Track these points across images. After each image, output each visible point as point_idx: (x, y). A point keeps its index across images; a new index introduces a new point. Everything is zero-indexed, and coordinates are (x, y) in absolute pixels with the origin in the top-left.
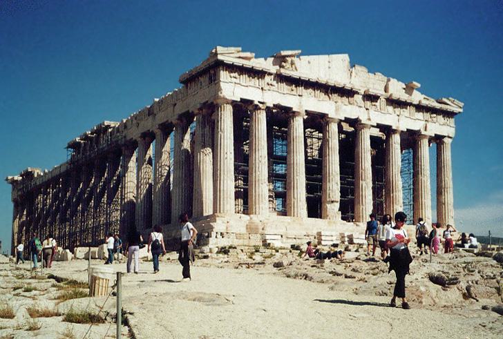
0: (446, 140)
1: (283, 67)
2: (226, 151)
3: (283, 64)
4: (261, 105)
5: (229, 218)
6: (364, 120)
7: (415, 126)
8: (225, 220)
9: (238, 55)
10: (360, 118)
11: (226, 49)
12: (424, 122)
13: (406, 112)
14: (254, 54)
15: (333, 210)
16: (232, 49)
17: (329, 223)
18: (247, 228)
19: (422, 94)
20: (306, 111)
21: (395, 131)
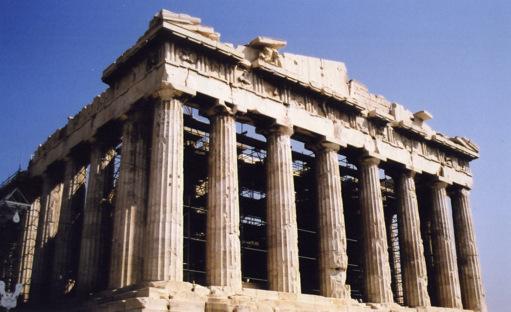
0: (464, 191)
1: (263, 59)
2: (169, 173)
4: (229, 109)
5: (174, 290)
6: (371, 149)
7: (433, 169)
8: (166, 292)
9: (195, 28)
10: (367, 148)
11: (177, 15)
12: (440, 165)
13: (419, 149)
14: (219, 35)
16: (185, 17)
20: (295, 127)
21: (408, 173)
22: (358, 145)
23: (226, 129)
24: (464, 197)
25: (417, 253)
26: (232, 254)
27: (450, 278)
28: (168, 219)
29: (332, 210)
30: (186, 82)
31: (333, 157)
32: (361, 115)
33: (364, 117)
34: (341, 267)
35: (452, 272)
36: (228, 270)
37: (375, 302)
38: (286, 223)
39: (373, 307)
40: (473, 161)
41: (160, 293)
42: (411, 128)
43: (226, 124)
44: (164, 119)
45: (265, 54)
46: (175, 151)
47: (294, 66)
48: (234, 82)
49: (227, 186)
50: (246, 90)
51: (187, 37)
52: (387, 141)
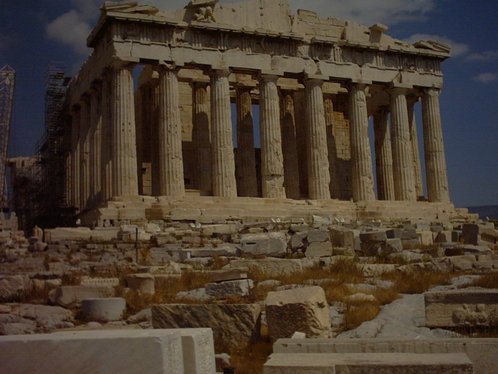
0: (431, 92)
1: (195, 19)
2: (122, 122)
3: (197, 15)
4: (168, 66)
9: (134, 9)
10: (307, 72)
12: (397, 72)
15: (275, 185)
17: (267, 202)
18: (146, 214)
19: (393, 38)
22: (297, 70)
23: (167, 82)
24: (431, 97)
25: (361, 155)
26: (174, 173)
27: (402, 175)
28: (122, 154)
29: (267, 129)
30: (131, 52)
31: (270, 85)
32: (304, 43)
33: (308, 44)
34: (274, 173)
35: (405, 169)
36: (171, 184)
37: (311, 199)
38: (222, 145)
39: (309, 204)
40: (446, 60)
41: (115, 204)
42: (358, 45)
43: (167, 78)
44: (117, 84)
45: (199, 13)
46: (125, 106)
47: (223, 20)
48: (173, 43)
49: (169, 125)
50: (184, 47)
51: (127, 19)
52: (334, 61)
